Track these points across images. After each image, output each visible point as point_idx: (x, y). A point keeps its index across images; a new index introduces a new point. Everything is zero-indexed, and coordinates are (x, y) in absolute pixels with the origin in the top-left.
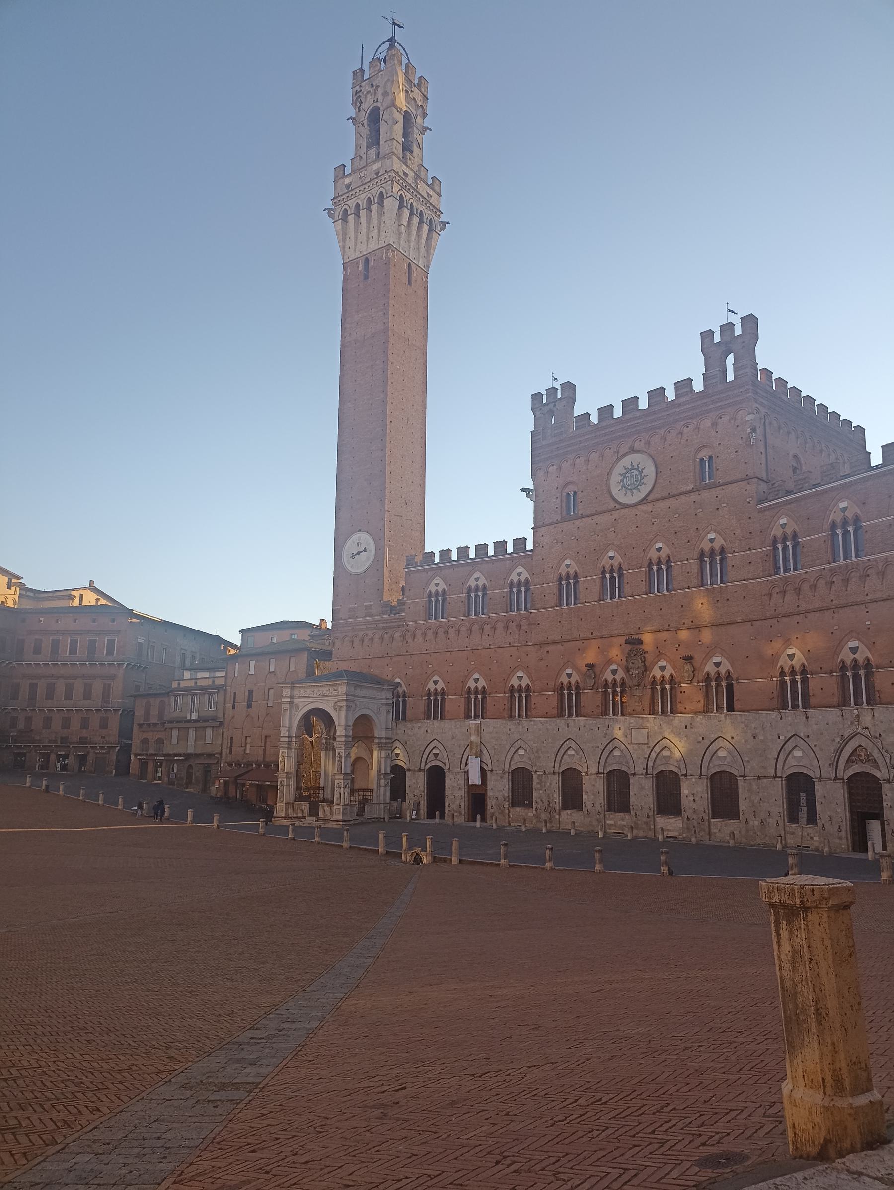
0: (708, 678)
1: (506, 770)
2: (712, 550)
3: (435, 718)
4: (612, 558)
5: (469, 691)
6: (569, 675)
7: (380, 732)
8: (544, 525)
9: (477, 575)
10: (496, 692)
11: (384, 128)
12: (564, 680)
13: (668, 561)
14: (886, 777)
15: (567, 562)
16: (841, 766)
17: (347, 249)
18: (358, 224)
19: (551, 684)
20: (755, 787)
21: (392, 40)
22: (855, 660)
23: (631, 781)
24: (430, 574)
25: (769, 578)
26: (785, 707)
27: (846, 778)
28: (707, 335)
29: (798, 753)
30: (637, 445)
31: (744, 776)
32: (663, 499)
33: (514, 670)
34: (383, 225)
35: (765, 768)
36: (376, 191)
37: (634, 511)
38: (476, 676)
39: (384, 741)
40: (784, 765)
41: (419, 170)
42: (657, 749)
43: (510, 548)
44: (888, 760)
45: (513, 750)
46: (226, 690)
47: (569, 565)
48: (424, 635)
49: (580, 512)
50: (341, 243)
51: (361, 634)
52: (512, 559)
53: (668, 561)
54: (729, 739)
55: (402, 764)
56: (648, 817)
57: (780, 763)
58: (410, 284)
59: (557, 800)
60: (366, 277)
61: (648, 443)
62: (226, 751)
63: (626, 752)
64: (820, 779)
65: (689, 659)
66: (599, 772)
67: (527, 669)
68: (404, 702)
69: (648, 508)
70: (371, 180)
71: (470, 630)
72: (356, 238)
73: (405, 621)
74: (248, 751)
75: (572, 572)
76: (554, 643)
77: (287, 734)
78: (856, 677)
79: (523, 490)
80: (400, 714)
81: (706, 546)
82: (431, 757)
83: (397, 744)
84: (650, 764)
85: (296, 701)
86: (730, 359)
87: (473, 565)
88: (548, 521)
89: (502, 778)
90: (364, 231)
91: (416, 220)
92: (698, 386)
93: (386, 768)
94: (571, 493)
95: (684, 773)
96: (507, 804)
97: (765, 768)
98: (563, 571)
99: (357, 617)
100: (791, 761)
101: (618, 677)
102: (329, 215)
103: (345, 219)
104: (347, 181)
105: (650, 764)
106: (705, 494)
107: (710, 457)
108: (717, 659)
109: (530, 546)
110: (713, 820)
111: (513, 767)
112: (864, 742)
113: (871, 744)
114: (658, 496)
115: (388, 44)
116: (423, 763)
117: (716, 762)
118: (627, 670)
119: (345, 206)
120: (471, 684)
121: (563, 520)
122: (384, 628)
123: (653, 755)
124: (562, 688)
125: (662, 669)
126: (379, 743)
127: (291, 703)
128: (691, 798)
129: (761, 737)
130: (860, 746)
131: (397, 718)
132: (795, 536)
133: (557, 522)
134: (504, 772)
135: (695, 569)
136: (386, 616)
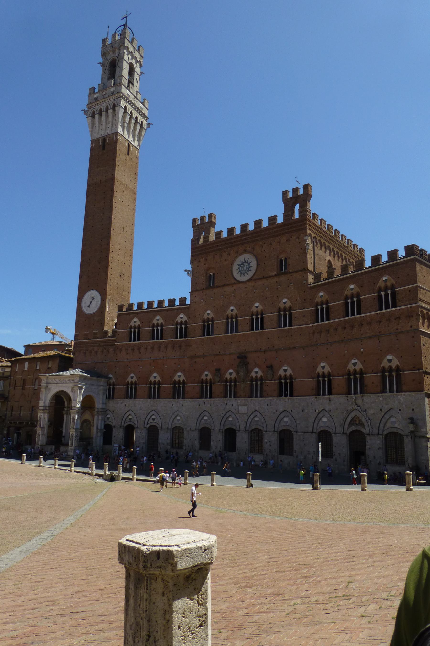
0: (280, 378)
1: (170, 427)
2: (285, 308)
3: (131, 398)
4: (232, 310)
5: (151, 383)
6: (207, 375)
7: (99, 405)
8: (196, 290)
9: (158, 317)
10: (166, 384)
11: (118, 70)
12: (204, 377)
14: (368, 432)
15: (208, 312)
16: (346, 426)
17: (94, 133)
18: (100, 119)
21: (124, 25)
23: (237, 434)
24: (131, 316)
25: (313, 325)
26: (319, 395)
27: (348, 433)
28: (285, 193)
29: (325, 419)
30: (248, 249)
31: (297, 432)
32: (260, 279)
33: (176, 371)
34: (114, 121)
38: (155, 374)
39: (101, 410)
40: (317, 426)
41: (137, 94)
42: (252, 417)
43: (177, 303)
44: (369, 423)
46: (10, 379)
48: (127, 350)
49: (216, 285)
50: (90, 129)
51: (90, 349)
52: (178, 309)
53: (262, 314)
54: (290, 411)
55: (110, 423)
56: (246, 454)
57: (316, 424)
58: (128, 154)
59: (197, 444)
61: (254, 248)
62: (9, 414)
64: (335, 433)
66: (220, 430)
67: (183, 371)
68: (114, 389)
69: (252, 284)
70: (109, 96)
71: (153, 348)
72: (99, 127)
73: (116, 342)
74: (22, 414)
75: (210, 318)
76: (199, 357)
77: (43, 405)
78: (355, 379)
79: (185, 271)
80: (111, 394)
81: (282, 306)
82: (128, 420)
83: (108, 412)
84: (248, 425)
85: (50, 386)
86: (297, 207)
87: (156, 312)
89: (167, 432)
90: (104, 123)
91: (133, 121)
92: (280, 220)
93: (101, 425)
94: (212, 274)
95: (265, 429)
96: (169, 447)
98: (206, 317)
99: (88, 339)
100: (321, 424)
101: (233, 377)
102: (85, 113)
103: (93, 116)
104: (96, 96)
105: (248, 425)
106: (283, 278)
107: (286, 259)
108: (285, 368)
109: (188, 302)
110: (280, 456)
111: (173, 426)
112: (358, 414)
113: (361, 415)
115: (123, 27)
116: (123, 423)
117: (283, 424)
118: (237, 373)
119: (94, 110)
120: (152, 379)
122: (104, 346)
123: (250, 420)
124: (202, 382)
125: (257, 372)
126: (98, 411)
127: (47, 387)
128: (268, 444)
129: (306, 411)
130: (356, 416)
131: (109, 398)
133: (204, 289)
135: (276, 319)
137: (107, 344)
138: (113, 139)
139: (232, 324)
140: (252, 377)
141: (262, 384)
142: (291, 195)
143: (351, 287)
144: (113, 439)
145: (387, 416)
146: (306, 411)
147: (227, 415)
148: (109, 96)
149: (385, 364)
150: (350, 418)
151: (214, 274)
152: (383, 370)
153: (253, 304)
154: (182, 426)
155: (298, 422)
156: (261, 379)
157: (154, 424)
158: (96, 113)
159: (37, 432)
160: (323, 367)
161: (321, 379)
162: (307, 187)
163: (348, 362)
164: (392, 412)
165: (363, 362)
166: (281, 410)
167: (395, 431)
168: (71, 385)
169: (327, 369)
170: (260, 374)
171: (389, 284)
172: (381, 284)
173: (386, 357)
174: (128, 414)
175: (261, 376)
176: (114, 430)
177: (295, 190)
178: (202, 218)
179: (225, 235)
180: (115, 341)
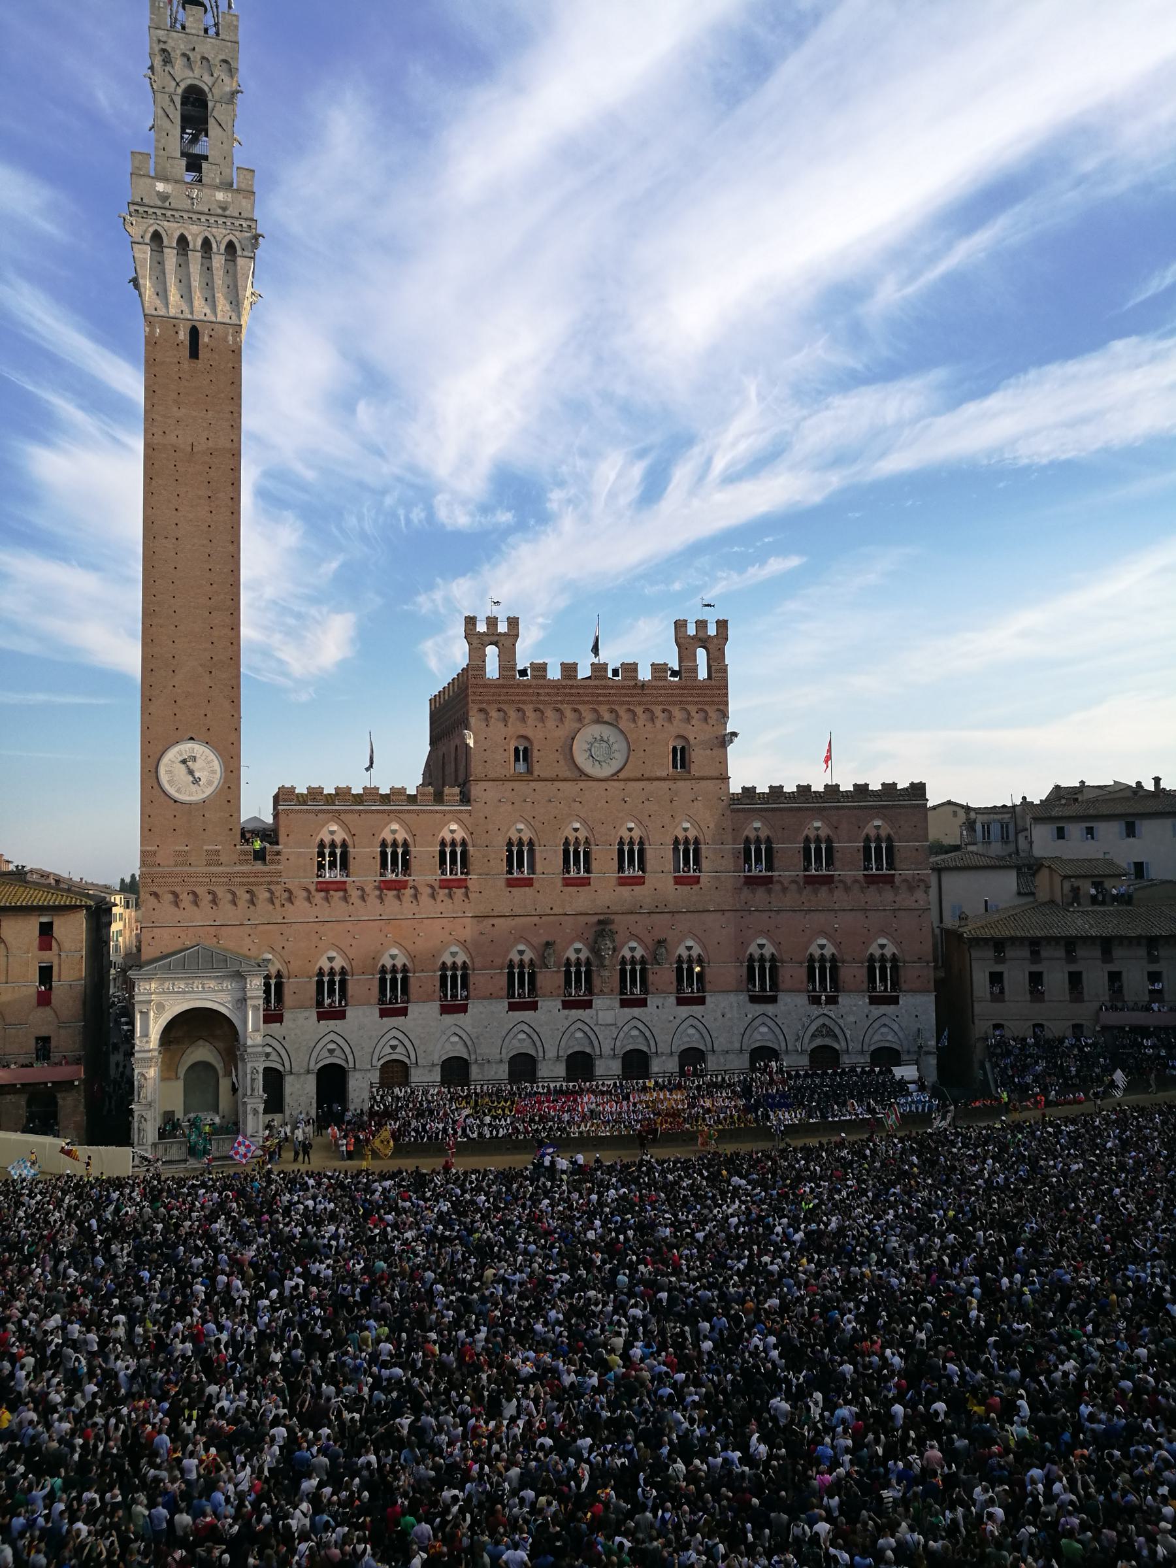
0: (680, 960)
13: (641, 843)
19: (498, 961)
20: (722, 1060)
22: (822, 955)
28: (680, 625)
29: (764, 1029)
35: (731, 1043)
36: (220, 235)
37: (604, 785)
42: (626, 1029)
45: (445, 1037)
47: (521, 830)
53: (641, 843)
60: (194, 353)
63: (590, 1033)
65: (661, 943)
69: (621, 785)
70: (209, 213)
82: (325, 1053)
88: (492, 775)
94: (521, 748)
97: (731, 1043)
101: (583, 956)
105: (618, 1044)
107: (683, 749)
108: (690, 943)
112: (827, 1022)
114: (632, 775)
118: (595, 950)
119: (156, 227)
121: (517, 778)
123: (622, 1035)
124: (511, 965)
125: (633, 949)
132: (769, 841)
134: (433, 1065)
136: (245, 868)
137: (252, 880)
138: (225, 340)
139: (577, 857)
140: (623, 957)
141: (643, 971)
142: (691, 630)
143: (818, 824)
144: (288, 1099)
145: (876, 1025)
146: (728, 1016)
147: (572, 1028)
148: (209, 213)
149: (874, 950)
150: (813, 1027)
151: (526, 749)
152: (872, 959)
153: (622, 825)
154: (466, 1056)
155: (714, 1035)
156: (643, 961)
157: (394, 1057)
158: (166, 242)
159: (136, 1114)
160: (761, 946)
161: (757, 965)
162: (722, 625)
163: (810, 942)
164: (885, 1020)
165: (838, 945)
166: (685, 1016)
167: (887, 1045)
168: (240, 995)
169: (769, 950)
170: (638, 954)
171: (883, 833)
172: (869, 830)
173: (876, 940)
174: (327, 1039)
175: (643, 957)
176: (288, 1080)
177: (702, 625)
178: (492, 622)
179: (554, 674)
180: (279, 874)
